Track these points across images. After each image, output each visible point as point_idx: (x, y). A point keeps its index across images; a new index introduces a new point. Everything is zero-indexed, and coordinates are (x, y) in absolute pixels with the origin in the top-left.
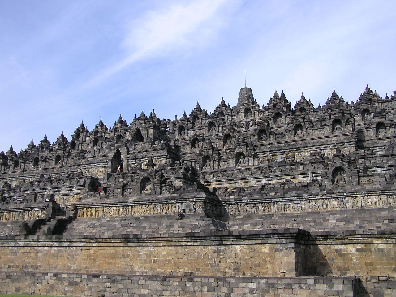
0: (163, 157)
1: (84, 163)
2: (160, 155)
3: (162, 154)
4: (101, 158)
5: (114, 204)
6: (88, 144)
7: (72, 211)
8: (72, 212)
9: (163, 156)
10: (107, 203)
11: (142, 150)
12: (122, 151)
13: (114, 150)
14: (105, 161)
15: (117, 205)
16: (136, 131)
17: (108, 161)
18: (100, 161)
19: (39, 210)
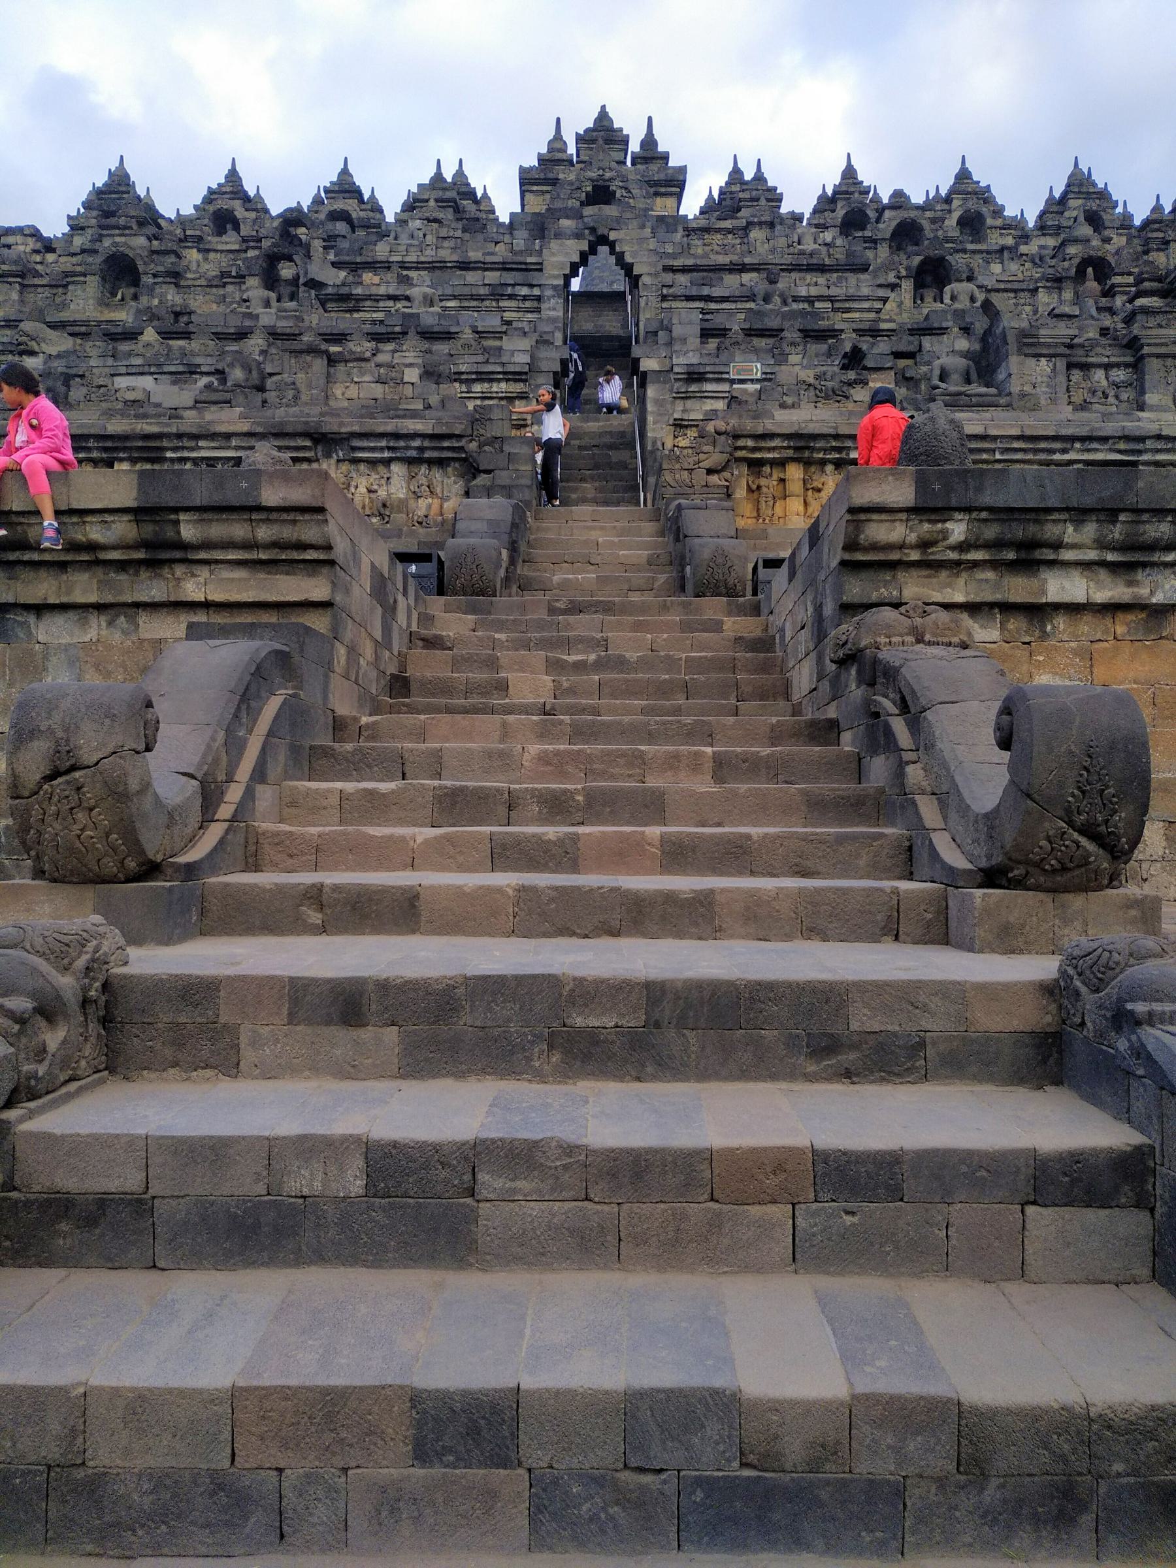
0: (866, 305)
1: (374, 290)
2: (851, 291)
3: (865, 291)
4: (492, 277)
5: (1043, 445)
6: (236, 247)
7: (710, 472)
8: (714, 479)
9: (867, 299)
10: (993, 432)
11: (735, 258)
12: (626, 248)
13: (578, 236)
14: (524, 291)
15: (1057, 457)
16: (587, 193)
17: (536, 291)
18: (483, 291)
19: (387, 462)
